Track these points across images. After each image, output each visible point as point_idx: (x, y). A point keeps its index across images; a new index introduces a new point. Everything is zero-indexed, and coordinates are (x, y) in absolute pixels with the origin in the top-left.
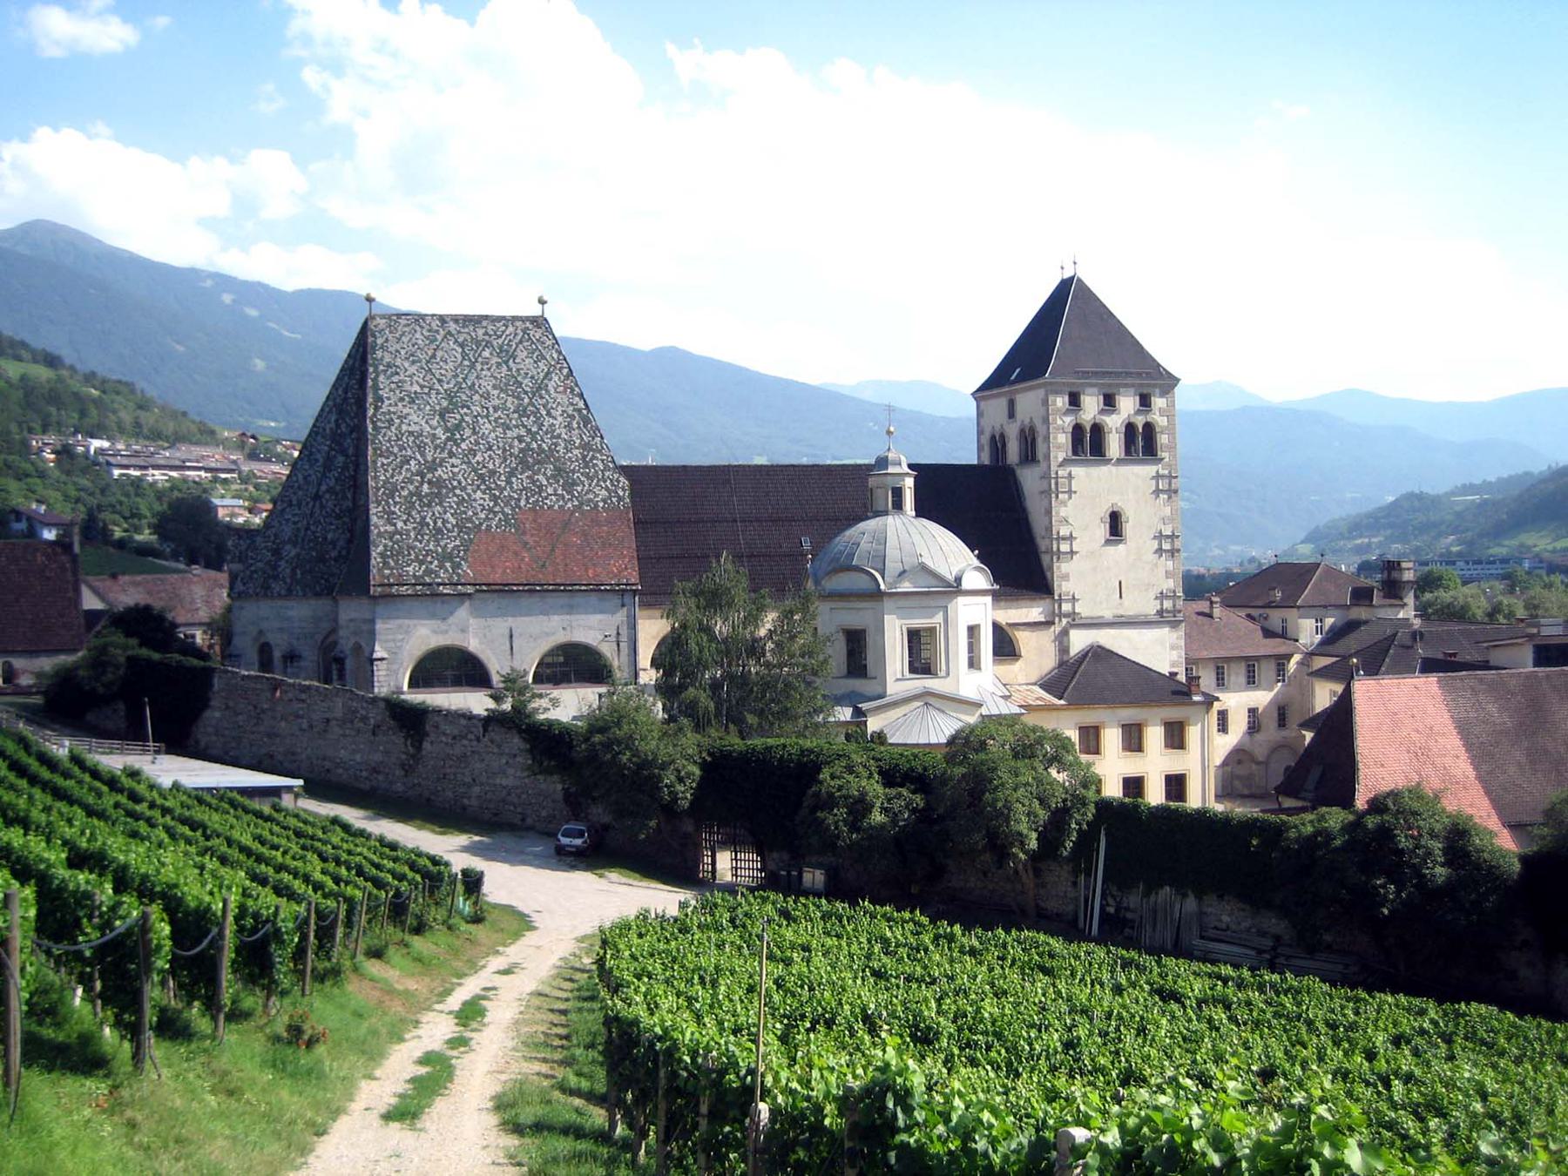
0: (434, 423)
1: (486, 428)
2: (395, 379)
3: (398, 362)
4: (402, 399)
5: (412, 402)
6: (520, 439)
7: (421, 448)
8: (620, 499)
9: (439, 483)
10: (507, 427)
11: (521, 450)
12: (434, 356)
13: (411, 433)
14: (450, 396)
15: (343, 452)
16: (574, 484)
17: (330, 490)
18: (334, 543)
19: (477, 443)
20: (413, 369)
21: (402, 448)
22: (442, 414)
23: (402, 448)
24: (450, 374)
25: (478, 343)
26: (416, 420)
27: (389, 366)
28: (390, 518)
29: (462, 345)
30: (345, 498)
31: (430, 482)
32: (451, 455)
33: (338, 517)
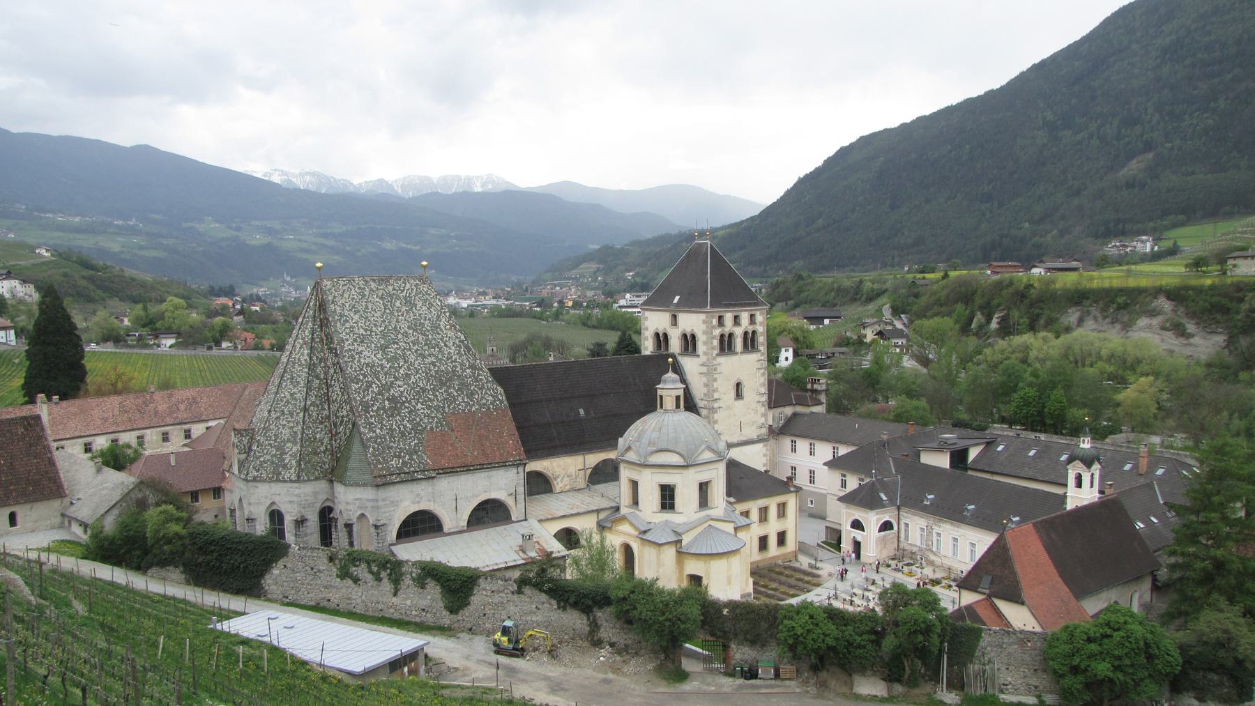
0: (379, 356)
1: (412, 358)
2: (347, 325)
3: (346, 312)
4: (355, 340)
5: (362, 342)
6: (433, 363)
7: (376, 374)
8: (502, 402)
9: (392, 400)
10: (424, 357)
11: (437, 372)
12: (367, 307)
13: (368, 365)
14: (384, 335)
15: (318, 377)
16: (472, 394)
17: (313, 404)
18: (321, 441)
19: (409, 369)
20: (356, 318)
21: (365, 376)
22: (384, 348)
23: (365, 376)
24: (380, 320)
25: (391, 296)
26: (369, 356)
27: (341, 315)
28: (371, 427)
29: (382, 298)
30: (323, 409)
31: (388, 399)
32: (396, 379)
33: (321, 423)
